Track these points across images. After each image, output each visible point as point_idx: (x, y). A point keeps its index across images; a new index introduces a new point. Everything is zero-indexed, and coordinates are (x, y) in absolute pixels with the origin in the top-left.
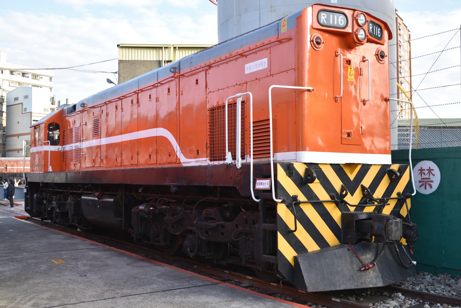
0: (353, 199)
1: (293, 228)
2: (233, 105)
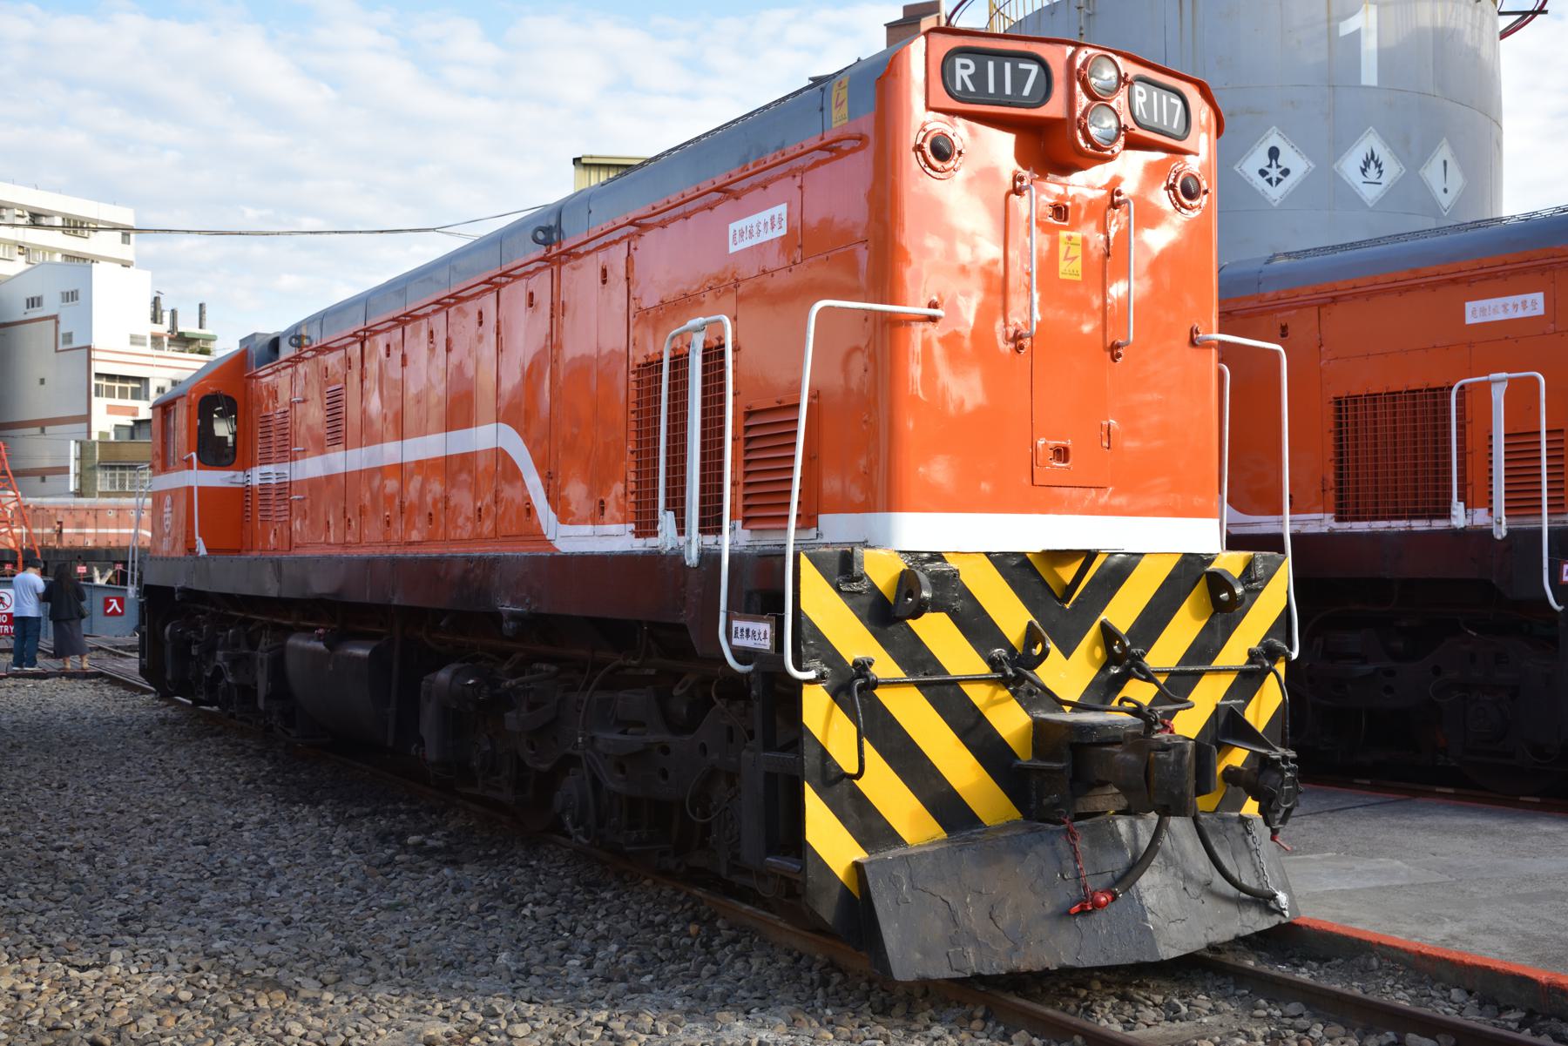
0: (1067, 673)
1: (850, 767)
2: (680, 362)
